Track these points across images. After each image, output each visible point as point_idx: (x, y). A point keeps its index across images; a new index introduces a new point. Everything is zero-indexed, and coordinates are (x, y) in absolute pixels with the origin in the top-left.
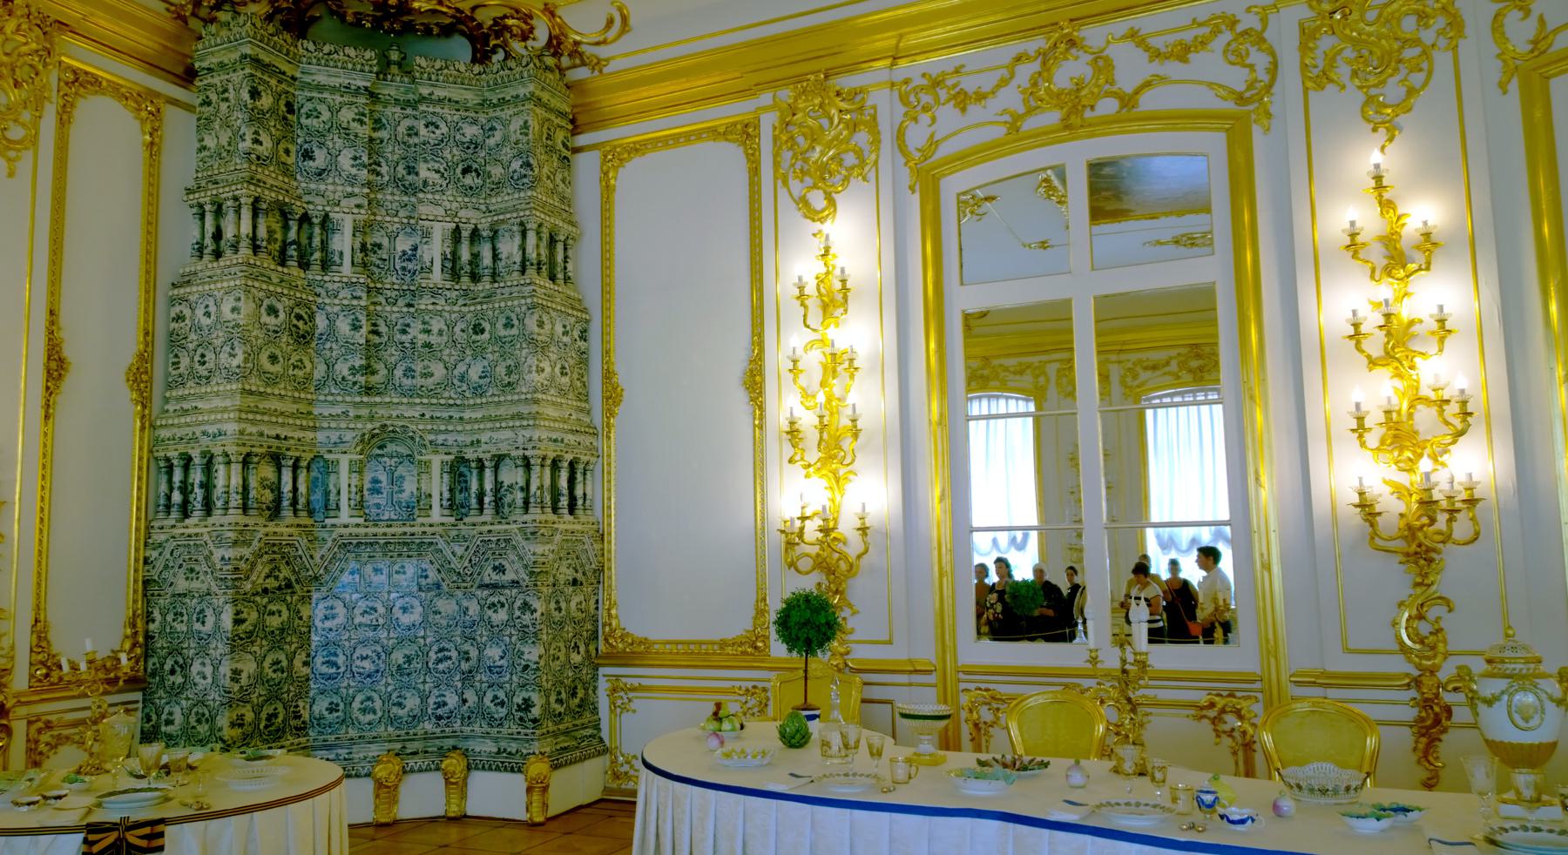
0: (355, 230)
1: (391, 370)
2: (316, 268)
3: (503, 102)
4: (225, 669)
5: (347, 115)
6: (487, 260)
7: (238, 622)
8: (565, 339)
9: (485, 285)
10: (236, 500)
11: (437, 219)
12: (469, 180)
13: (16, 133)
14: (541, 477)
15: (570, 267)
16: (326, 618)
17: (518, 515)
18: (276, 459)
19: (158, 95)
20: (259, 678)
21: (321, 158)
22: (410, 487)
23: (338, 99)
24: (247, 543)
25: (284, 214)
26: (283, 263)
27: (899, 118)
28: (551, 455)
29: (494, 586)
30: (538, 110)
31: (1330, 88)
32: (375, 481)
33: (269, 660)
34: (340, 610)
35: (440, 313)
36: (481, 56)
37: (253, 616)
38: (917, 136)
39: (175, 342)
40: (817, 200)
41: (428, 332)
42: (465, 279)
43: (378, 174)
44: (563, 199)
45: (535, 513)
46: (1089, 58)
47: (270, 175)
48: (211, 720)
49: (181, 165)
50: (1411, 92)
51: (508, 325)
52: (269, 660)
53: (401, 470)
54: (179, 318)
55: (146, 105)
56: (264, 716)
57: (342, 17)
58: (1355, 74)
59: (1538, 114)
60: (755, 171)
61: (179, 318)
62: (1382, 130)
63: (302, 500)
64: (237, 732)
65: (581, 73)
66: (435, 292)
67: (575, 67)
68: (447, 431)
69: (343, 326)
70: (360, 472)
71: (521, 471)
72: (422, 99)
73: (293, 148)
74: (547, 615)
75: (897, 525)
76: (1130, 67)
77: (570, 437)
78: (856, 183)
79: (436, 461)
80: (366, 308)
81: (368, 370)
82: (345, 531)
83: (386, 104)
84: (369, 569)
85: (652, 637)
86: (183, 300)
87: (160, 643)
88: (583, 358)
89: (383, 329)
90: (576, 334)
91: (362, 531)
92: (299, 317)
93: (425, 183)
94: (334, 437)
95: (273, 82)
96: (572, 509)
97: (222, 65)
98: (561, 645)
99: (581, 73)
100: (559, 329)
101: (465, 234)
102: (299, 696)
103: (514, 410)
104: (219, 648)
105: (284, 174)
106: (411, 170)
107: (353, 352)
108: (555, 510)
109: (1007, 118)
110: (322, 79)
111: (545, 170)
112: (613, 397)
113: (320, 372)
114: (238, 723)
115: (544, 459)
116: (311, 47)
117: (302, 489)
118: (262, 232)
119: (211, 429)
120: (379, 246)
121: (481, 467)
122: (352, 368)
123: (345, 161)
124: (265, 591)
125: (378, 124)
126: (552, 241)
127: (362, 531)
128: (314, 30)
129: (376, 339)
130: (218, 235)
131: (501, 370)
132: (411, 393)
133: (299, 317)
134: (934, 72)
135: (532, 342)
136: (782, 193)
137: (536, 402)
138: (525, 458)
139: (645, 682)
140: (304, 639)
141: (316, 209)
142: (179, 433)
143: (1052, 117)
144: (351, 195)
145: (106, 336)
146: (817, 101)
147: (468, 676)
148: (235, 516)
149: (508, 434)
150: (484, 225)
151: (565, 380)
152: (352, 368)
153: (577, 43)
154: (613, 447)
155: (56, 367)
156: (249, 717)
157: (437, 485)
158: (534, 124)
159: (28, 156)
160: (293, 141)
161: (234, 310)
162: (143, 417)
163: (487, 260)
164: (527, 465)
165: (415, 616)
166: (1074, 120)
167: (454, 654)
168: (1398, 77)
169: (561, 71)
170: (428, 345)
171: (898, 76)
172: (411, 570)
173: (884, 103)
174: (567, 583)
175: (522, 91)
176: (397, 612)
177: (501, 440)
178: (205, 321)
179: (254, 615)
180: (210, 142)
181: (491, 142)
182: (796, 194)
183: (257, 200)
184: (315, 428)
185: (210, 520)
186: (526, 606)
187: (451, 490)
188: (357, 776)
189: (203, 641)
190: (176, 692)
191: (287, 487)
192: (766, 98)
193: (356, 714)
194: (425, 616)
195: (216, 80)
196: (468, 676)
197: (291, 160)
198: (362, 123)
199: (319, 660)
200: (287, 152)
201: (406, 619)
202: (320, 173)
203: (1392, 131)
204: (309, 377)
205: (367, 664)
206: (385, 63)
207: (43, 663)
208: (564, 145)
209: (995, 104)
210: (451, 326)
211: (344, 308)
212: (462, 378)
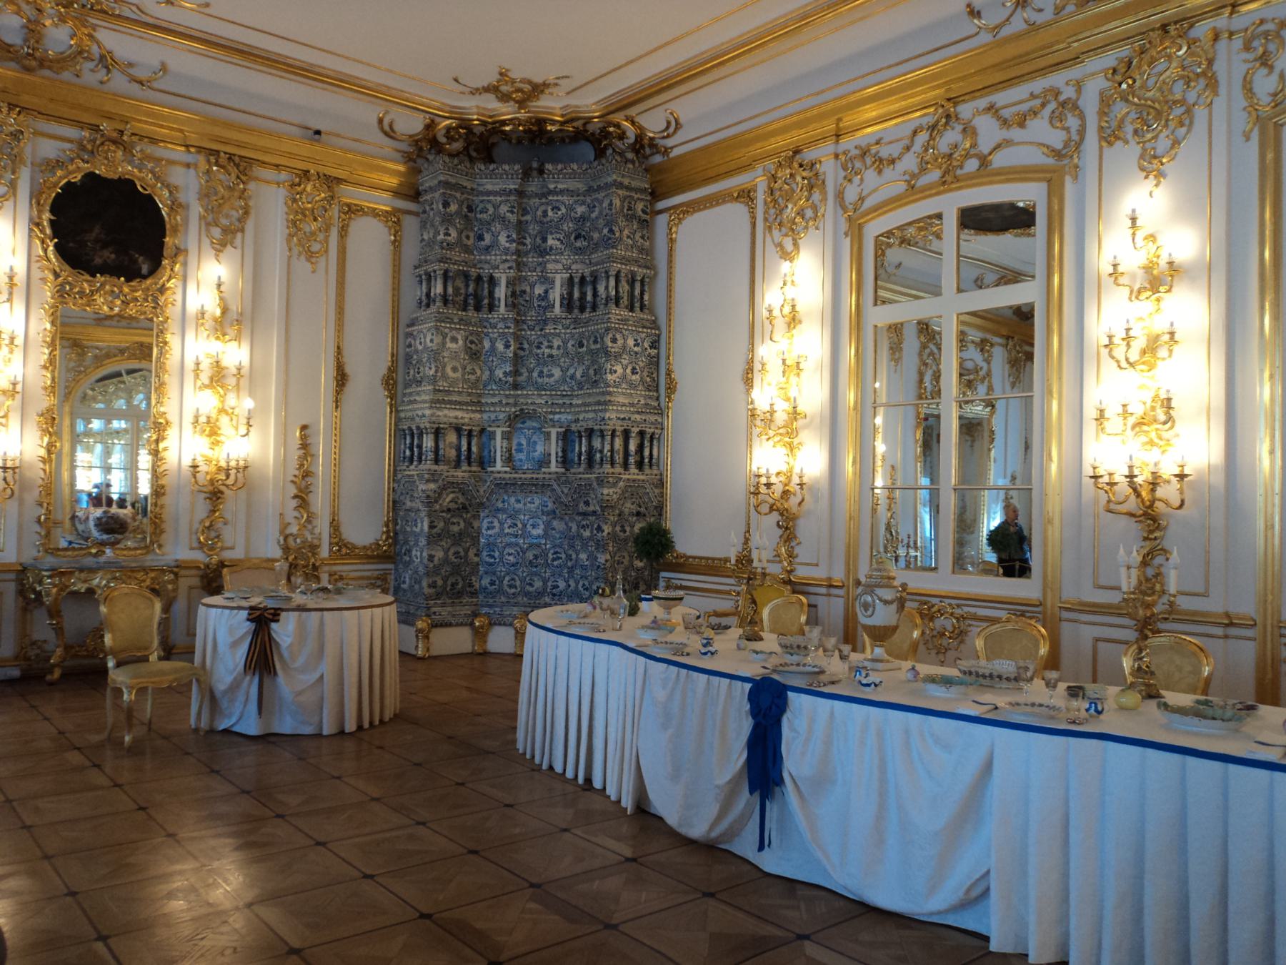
0: (508, 283)
1: (530, 372)
2: (485, 310)
3: (599, 188)
4: (425, 554)
5: (504, 209)
6: (589, 298)
7: (431, 527)
8: (636, 349)
9: (586, 315)
10: (431, 456)
11: (559, 271)
12: (578, 244)
13: (316, 247)
14: (612, 444)
15: (646, 297)
16: (488, 528)
17: (597, 469)
18: (458, 430)
19: (400, 210)
20: (446, 561)
21: (488, 237)
22: (540, 448)
23: (499, 199)
24: (435, 481)
25: (466, 276)
26: (465, 310)
27: (840, 180)
28: (619, 429)
29: (584, 514)
30: (620, 192)
31: (1119, 144)
32: (520, 444)
33: (452, 551)
34: (496, 524)
35: (558, 335)
36: (600, 153)
37: (442, 524)
38: (851, 194)
39: (408, 358)
40: (789, 246)
41: (551, 347)
42: (576, 311)
43: (525, 244)
44: (641, 250)
45: (607, 468)
46: (961, 127)
47: (457, 255)
48: (420, 582)
49: (411, 252)
50: (1176, 143)
51: (595, 342)
52: (452, 551)
53: (535, 438)
54: (410, 346)
55: (394, 219)
56: (449, 583)
57: (510, 141)
58: (1136, 132)
59: (1270, 156)
60: (754, 225)
61: (410, 346)
62: (1151, 177)
63: (474, 456)
64: (432, 591)
65: (658, 159)
66: (556, 321)
67: (653, 154)
68: (560, 413)
69: (500, 346)
70: (509, 439)
71: (599, 439)
72: (551, 192)
73: (472, 235)
74: (613, 536)
75: (825, 484)
76: (988, 131)
77: (638, 417)
78: (811, 230)
79: (554, 432)
80: (514, 334)
81: (516, 373)
82: (498, 476)
83: (530, 197)
84: (513, 500)
85: (689, 554)
86: (410, 335)
87: (401, 537)
88: (654, 362)
89: (526, 346)
90: (646, 345)
91: (507, 476)
92: (472, 342)
93: (551, 248)
94: (493, 417)
95: (458, 195)
96: (640, 465)
97: (430, 188)
98: (626, 554)
99: (658, 159)
100: (631, 342)
101: (577, 280)
102: (472, 573)
103: (597, 399)
104: (423, 542)
105: (466, 252)
106: (544, 240)
107: (505, 362)
108: (626, 465)
109: (907, 177)
110: (489, 187)
111: (626, 232)
112: (671, 388)
113: (486, 376)
114: (433, 585)
115: (614, 431)
116: (483, 168)
117: (474, 449)
118: (450, 290)
119: (420, 413)
120: (524, 292)
121: (580, 437)
122: (505, 373)
123: (502, 239)
124: (449, 510)
125: (525, 212)
126: (632, 283)
127: (507, 476)
128: (496, 153)
129: (522, 353)
130: (428, 295)
131: (591, 372)
132: (540, 388)
133: (472, 342)
134: (863, 144)
135: (607, 353)
136: (768, 240)
137: (610, 393)
138: (602, 431)
139: (684, 583)
140: (475, 541)
141: (486, 272)
142: (410, 414)
143: (934, 175)
144: (506, 261)
145: (370, 357)
146: (788, 171)
147: (571, 570)
148: (428, 465)
149: (591, 415)
150: (587, 272)
151: (634, 377)
152: (505, 373)
153: (652, 139)
154: (669, 423)
155: (341, 378)
156: (440, 582)
157: (554, 448)
158: (617, 202)
159: (323, 259)
160: (472, 229)
161: (432, 341)
162: (391, 405)
163: (589, 298)
164: (603, 436)
165: (539, 531)
166: (948, 178)
167: (563, 556)
168: (1165, 133)
169: (646, 157)
170: (551, 356)
171: (841, 148)
172: (537, 502)
173: (829, 169)
174: (631, 514)
175: (610, 180)
176: (529, 528)
177: (588, 419)
178: (420, 348)
179: (442, 524)
180: (426, 237)
181: (593, 215)
182: (776, 241)
183: (446, 273)
184: (481, 412)
185: (421, 467)
186: (599, 529)
187: (564, 451)
188: (505, 624)
189: (417, 535)
190: (407, 564)
191: (464, 448)
192: (760, 171)
193: (506, 588)
194: (545, 531)
195: (428, 197)
196: (571, 570)
197: (470, 243)
198: (512, 212)
199: (485, 553)
200: (468, 237)
201: (535, 532)
202: (487, 249)
203: (1160, 175)
204: (478, 380)
205: (511, 558)
206: (526, 174)
207: (337, 544)
208: (643, 211)
209: (901, 166)
210: (565, 342)
211: (501, 335)
212: (572, 377)
